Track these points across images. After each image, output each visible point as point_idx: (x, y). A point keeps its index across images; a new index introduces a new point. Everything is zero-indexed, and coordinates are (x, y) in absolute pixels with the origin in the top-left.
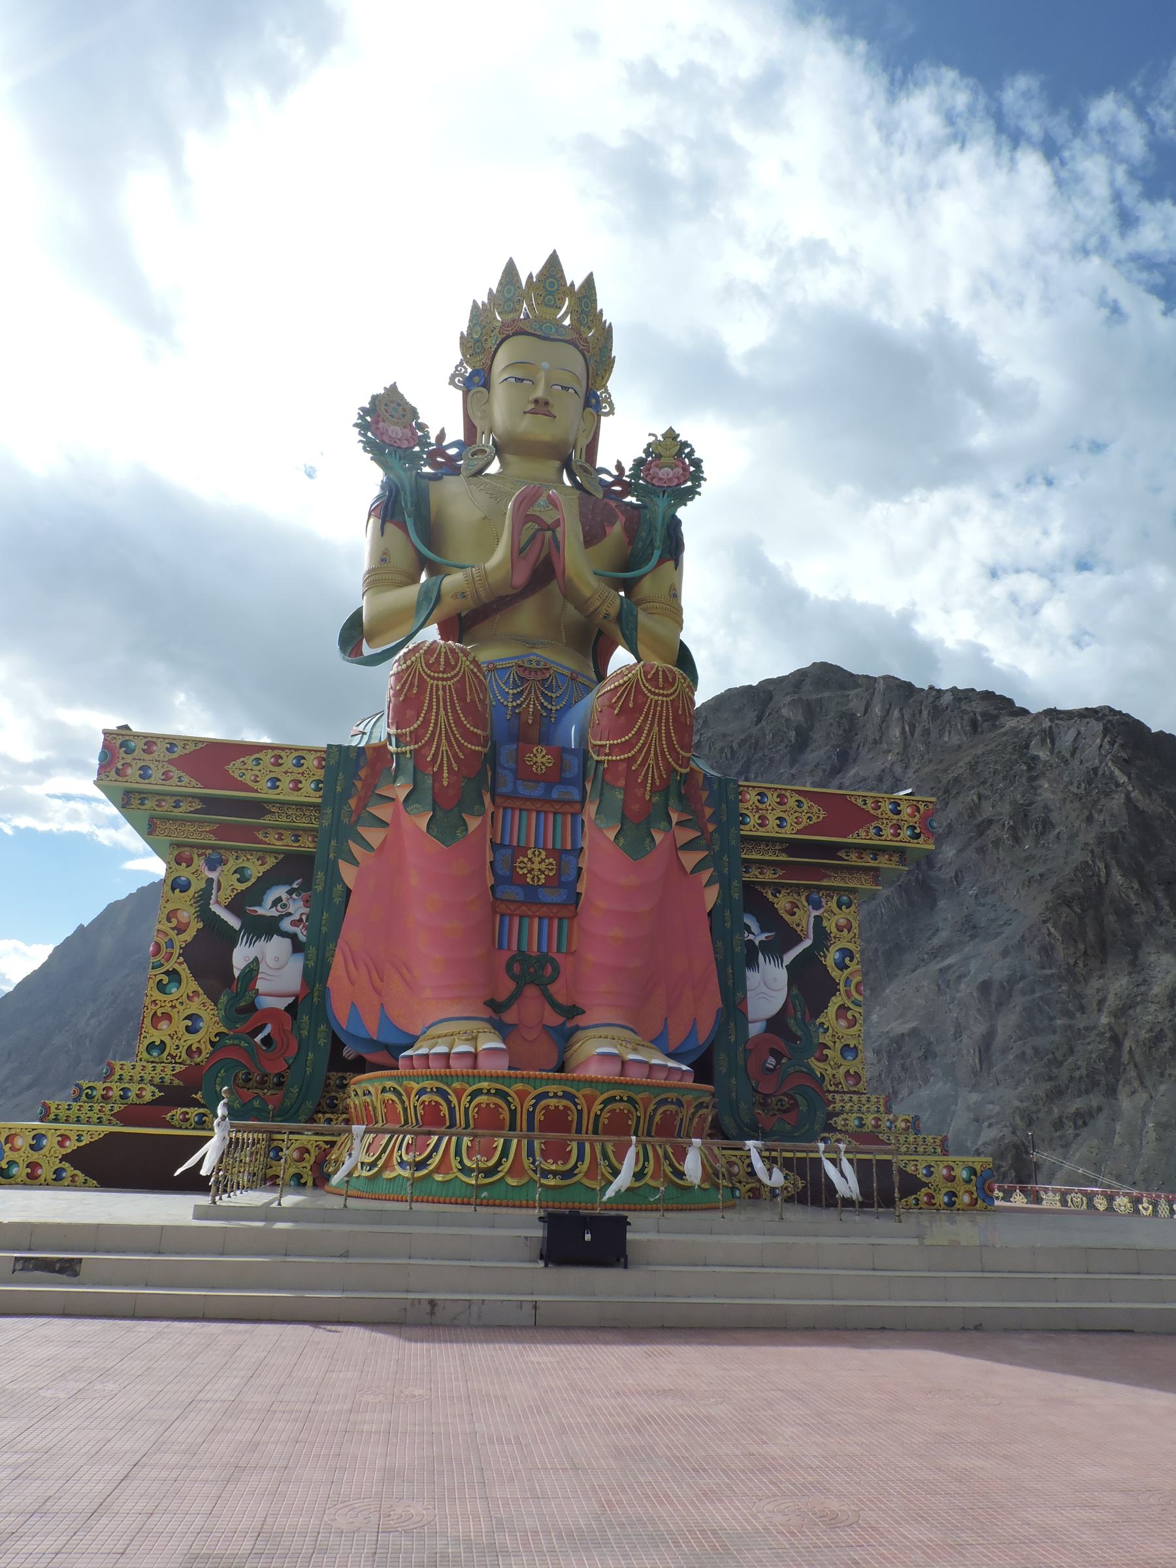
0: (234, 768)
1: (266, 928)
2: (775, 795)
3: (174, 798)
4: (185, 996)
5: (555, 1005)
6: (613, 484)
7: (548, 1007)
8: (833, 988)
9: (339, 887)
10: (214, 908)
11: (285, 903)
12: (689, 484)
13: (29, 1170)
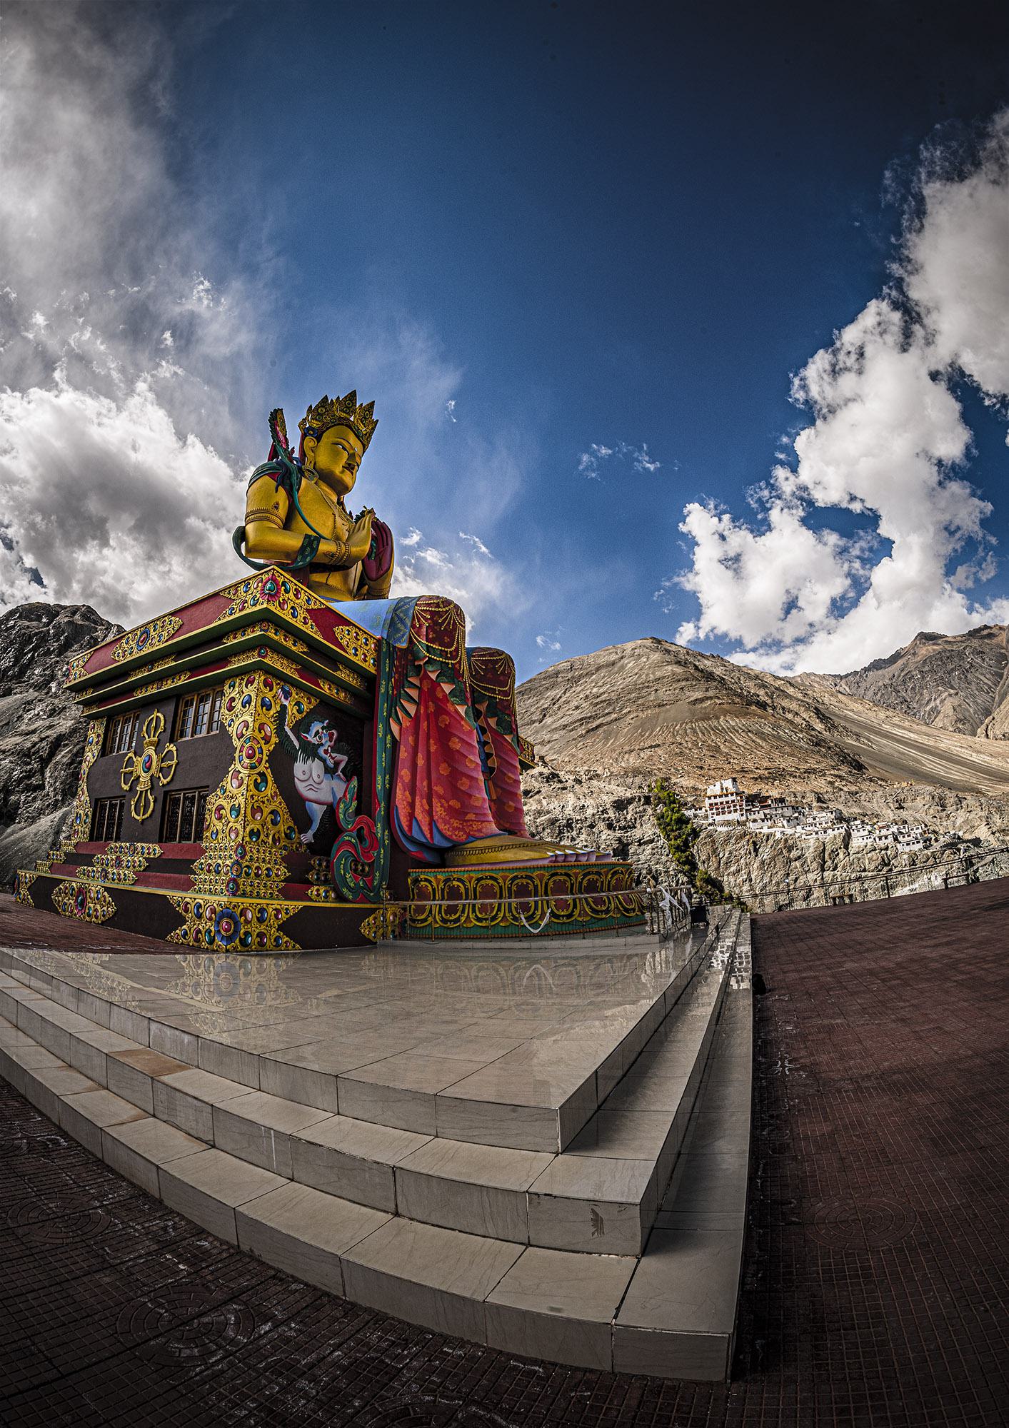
0: (337, 630)
1: (311, 751)
10: (287, 729)
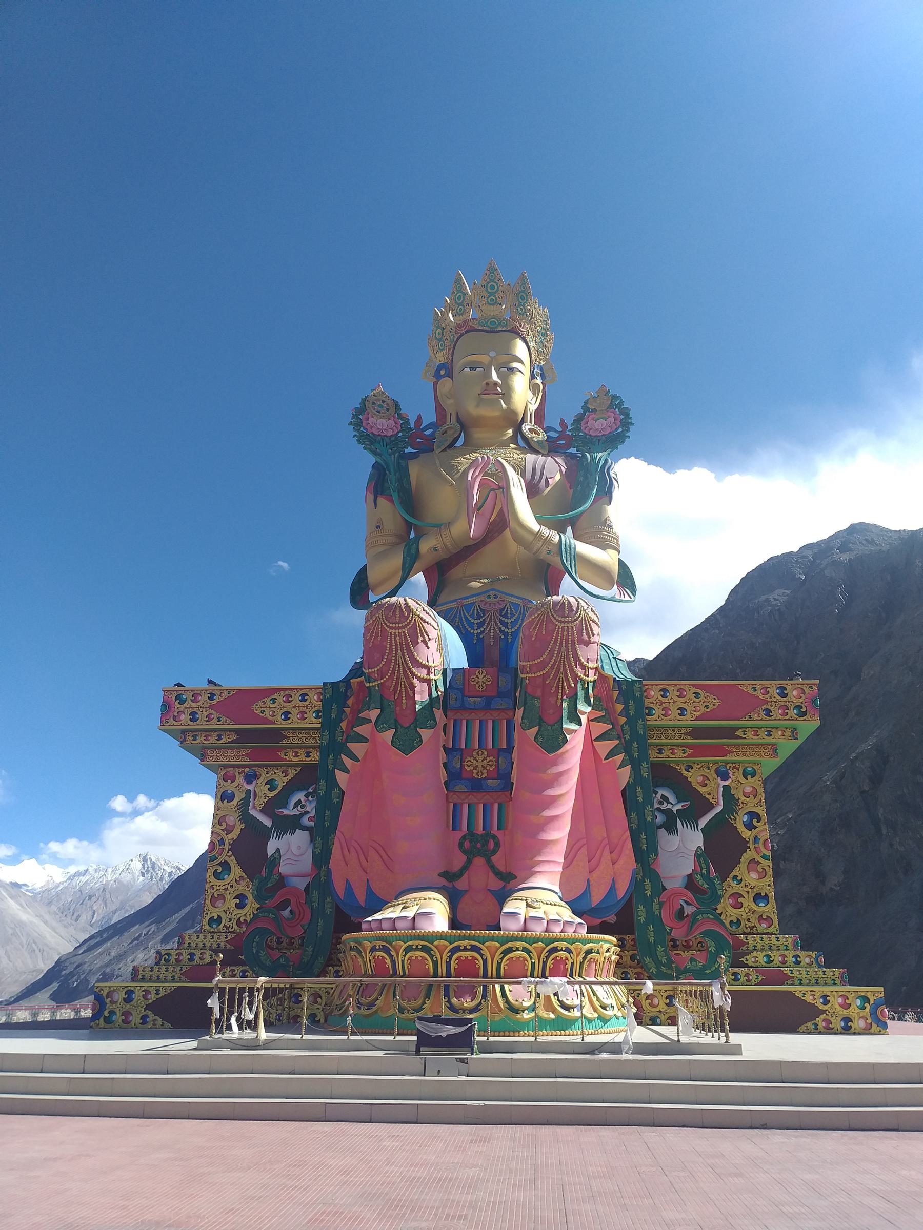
0: (257, 709)
1: (288, 825)
2: (676, 690)
3: (217, 733)
4: (234, 881)
5: (498, 874)
6: (559, 439)
7: (491, 874)
8: (743, 846)
9: (336, 790)
10: (252, 812)
11: (302, 804)
12: (620, 430)
13: (123, 1017)
